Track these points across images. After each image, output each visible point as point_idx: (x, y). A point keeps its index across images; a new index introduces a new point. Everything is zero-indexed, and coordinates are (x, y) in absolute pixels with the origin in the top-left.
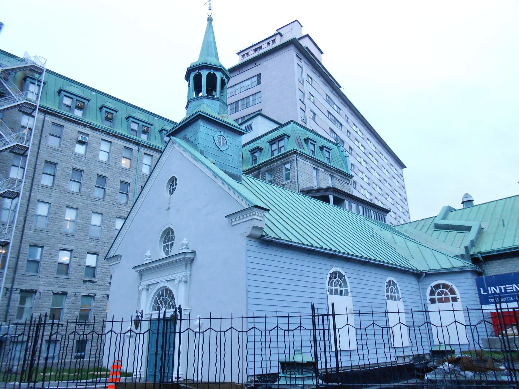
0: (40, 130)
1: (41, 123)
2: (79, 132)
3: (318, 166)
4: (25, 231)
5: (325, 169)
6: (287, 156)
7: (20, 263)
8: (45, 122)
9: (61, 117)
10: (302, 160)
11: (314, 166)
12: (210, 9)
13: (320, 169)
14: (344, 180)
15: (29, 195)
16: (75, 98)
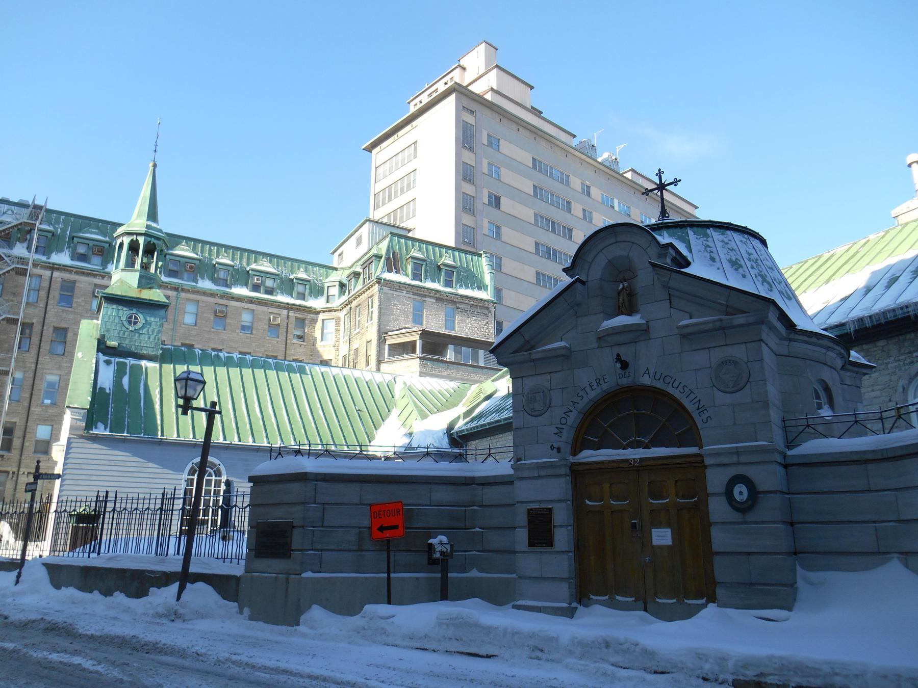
0: (47, 291)
1: (48, 283)
2: (96, 285)
3: (424, 296)
4: (32, 409)
5: (438, 299)
6: (372, 286)
7: (27, 444)
8: (53, 279)
9: (73, 271)
10: (391, 292)
11: (416, 297)
12: (155, 151)
13: (427, 299)
14: (478, 310)
15: (34, 368)
16: (91, 243)
